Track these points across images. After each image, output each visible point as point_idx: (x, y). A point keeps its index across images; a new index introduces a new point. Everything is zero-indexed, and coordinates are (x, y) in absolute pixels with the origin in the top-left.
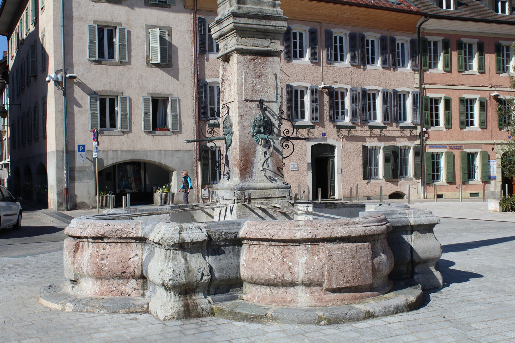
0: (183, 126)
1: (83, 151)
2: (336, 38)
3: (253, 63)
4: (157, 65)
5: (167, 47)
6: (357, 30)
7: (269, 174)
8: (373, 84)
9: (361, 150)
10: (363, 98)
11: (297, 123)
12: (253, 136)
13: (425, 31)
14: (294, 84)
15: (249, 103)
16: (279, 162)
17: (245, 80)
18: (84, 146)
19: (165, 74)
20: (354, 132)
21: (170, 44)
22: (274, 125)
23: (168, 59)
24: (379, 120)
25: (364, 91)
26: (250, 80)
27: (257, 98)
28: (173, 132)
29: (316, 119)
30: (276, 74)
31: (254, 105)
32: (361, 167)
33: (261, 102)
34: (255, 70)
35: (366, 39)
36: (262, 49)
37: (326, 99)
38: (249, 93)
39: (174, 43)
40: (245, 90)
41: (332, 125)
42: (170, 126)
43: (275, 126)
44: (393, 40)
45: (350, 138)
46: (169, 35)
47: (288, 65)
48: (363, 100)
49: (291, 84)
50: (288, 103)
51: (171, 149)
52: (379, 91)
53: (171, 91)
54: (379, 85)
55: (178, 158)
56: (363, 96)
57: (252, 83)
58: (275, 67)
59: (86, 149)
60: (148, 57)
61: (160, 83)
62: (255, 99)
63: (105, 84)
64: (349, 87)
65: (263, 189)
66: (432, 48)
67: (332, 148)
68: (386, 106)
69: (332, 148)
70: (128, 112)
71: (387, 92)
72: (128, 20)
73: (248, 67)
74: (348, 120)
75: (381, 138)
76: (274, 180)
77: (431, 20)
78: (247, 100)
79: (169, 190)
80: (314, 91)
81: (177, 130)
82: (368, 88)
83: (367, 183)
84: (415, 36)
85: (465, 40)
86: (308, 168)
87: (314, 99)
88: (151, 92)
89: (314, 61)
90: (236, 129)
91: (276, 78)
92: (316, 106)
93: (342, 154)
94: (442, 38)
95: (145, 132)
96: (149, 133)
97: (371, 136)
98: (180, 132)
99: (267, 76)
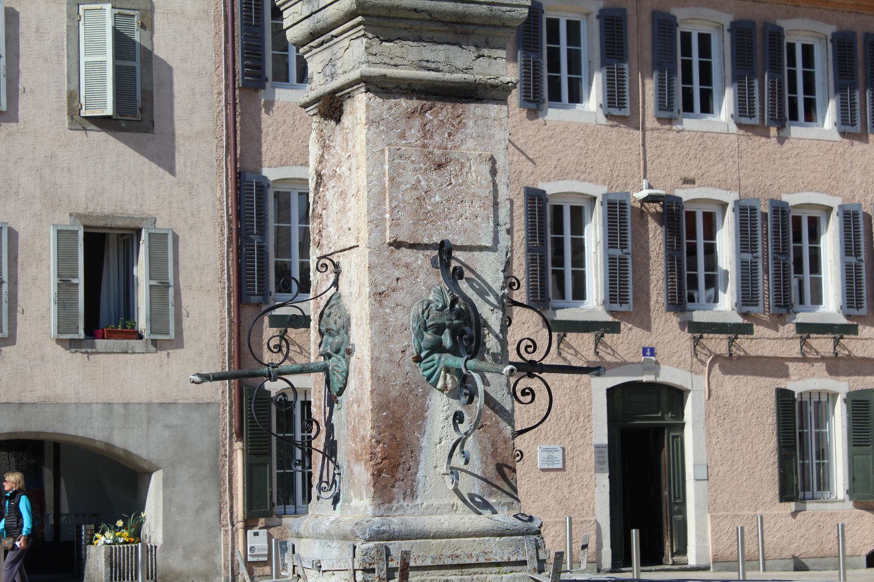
0: (186, 323)
3: (417, 122)
4: (102, 123)
5: (137, 64)
6: (758, 13)
7: (470, 485)
8: (809, 187)
9: (771, 403)
10: (776, 233)
11: (562, 315)
12: (418, 359)
14: (551, 188)
15: (405, 255)
16: (501, 445)
17: (392, 179)
19: (129, 152)
20: (747, 345)
21: (148, 55)
22: (486, 324)
23: (139, 105)
24: (831, 306)
25: (780, 210)
26: (409, 177)
27: (430, 236)
28: (154, 342)
29: (624, 300)
30: (493, 160)
31: (421, 260)
32: (774, 458)
33: (445, 250)
34: (424, 146)
35: (788, 39)
36: (448, 77)
37: (656, 237)
38: (407, 222)
39: (160, 51)
40: (393, 209)
41: (674, 320)
42: (142, 323)
43: (489, 328)
45: (734, 364)
46: (143, 26)
47: (532, 126)
48: (776, 240)
49: (541, 186)
50: (529, 250)
51: (144, 400)
52: (828, 210)
53: (149, 209)
54: (830, 191)
55: (168, 427)
56: (776, 226)
57: (415, 188)
58: (491, 137)
60: (73, 95)
61: (114, 180)
62: (426, 241)
64: (730, 197)
65: (448, 535)
67: (675, 397)
68: (853, 260)
69: (675, 397)
70: (5, 277)
71: (856, 215)
73: (403, 136)
74: (726, 305)
75: (837, 365)
76: (486, 505)
78: (397, 244)
79: (137, 535)
80: (616, 211)
81: (167, 337)
82: (792, 199)
83: (794, 514)
86: (598, 462)
87: (615, 235)
88: (81, 210)
89: (615, 112)
90: (361, 337)
91: (494, 172)
92: (623, 260)
93: (708, 415)
95: (59, 341)
96: (73, 345)
97: (804, 359)
98: (178, 342)
99: (462, 166)
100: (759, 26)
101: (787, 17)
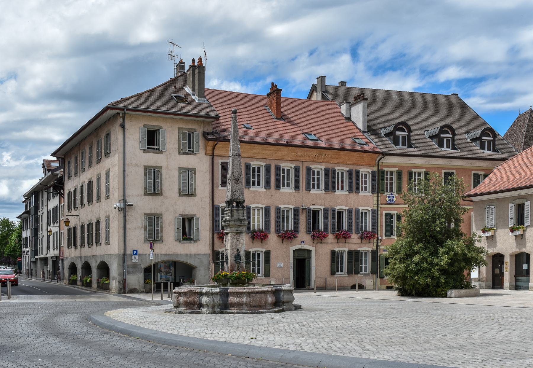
1: (136, 254)
2: (314, 172)
13: (384, 164)
18: (137, 251)
44: (358, 172)
59: (138, 253)
60: (180, 190)
61: (187, 206)
63: (151, 209)
66: (389, 176)
72: (168, 165)
77: (386, 157)
84: (375, 169)
85: (414, 170)
90: (229, 258)
94: (397, 169)
100: (331, 169)
101: (337, 166)
